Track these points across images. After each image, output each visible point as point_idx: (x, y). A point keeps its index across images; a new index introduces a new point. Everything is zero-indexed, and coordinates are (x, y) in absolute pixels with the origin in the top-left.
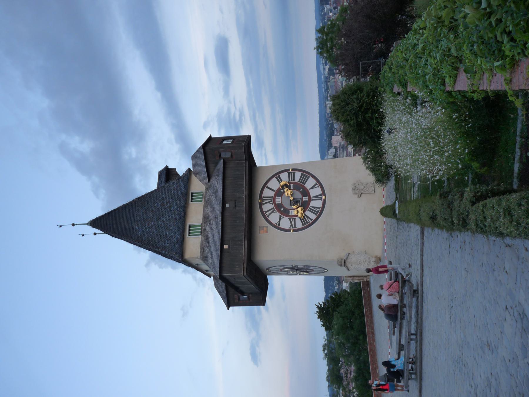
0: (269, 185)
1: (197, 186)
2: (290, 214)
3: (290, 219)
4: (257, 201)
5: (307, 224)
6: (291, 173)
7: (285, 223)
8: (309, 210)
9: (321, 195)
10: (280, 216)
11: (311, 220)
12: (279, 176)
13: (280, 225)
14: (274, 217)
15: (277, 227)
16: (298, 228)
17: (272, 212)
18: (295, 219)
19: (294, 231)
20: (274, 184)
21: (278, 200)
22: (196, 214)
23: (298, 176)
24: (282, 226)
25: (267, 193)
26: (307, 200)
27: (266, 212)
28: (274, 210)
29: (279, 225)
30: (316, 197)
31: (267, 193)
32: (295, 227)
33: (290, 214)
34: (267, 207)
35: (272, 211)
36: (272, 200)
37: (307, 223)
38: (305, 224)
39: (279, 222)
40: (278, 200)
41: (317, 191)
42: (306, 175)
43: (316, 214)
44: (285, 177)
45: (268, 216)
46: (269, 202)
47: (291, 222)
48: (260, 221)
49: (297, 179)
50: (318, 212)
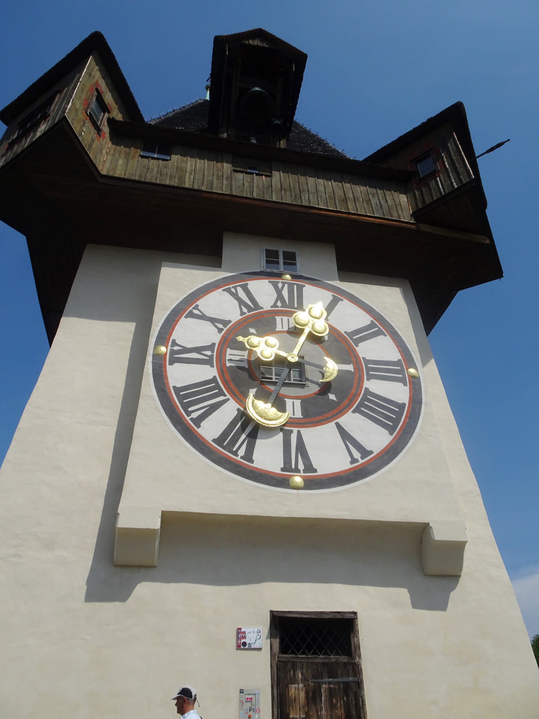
2: (229, 351)
9: (309, 468)
10: (225, 323)
11: (198, 421)
13: (190, 320)
17: (241, 302)
28: (250, 309)
30: (301, 447)
33: (229, 351)
37: (185, 407)
38: (181, 398)
39: (203, 317)
43: (219, 441)
45: (228, 291)
46: (280, 297)
47: (198, 350)
49: (375, 386)
50: (229, 447)
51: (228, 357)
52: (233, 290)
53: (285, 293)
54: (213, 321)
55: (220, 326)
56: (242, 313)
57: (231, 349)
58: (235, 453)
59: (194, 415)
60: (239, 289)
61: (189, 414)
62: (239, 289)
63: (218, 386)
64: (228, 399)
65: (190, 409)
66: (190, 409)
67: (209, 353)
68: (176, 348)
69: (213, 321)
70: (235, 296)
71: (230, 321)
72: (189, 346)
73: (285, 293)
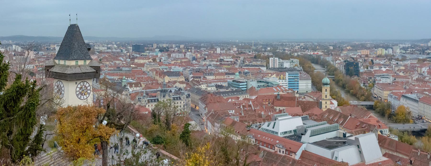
1: (88, 62)
4: (83, 81)
5: (77, 95)
7: (78, 89)
14: (79, 86)
15: (77, 87)
20: (87, 85)
21: (83, 87)
22: (81, 63)
23: (89, 92)
25: (85, 83)
31: (85, 83)
34: (82, 83)
36: (84, 84)
40: (83, 87)
41: (85, 97)
42: (89, 94)
48: (78, 82)
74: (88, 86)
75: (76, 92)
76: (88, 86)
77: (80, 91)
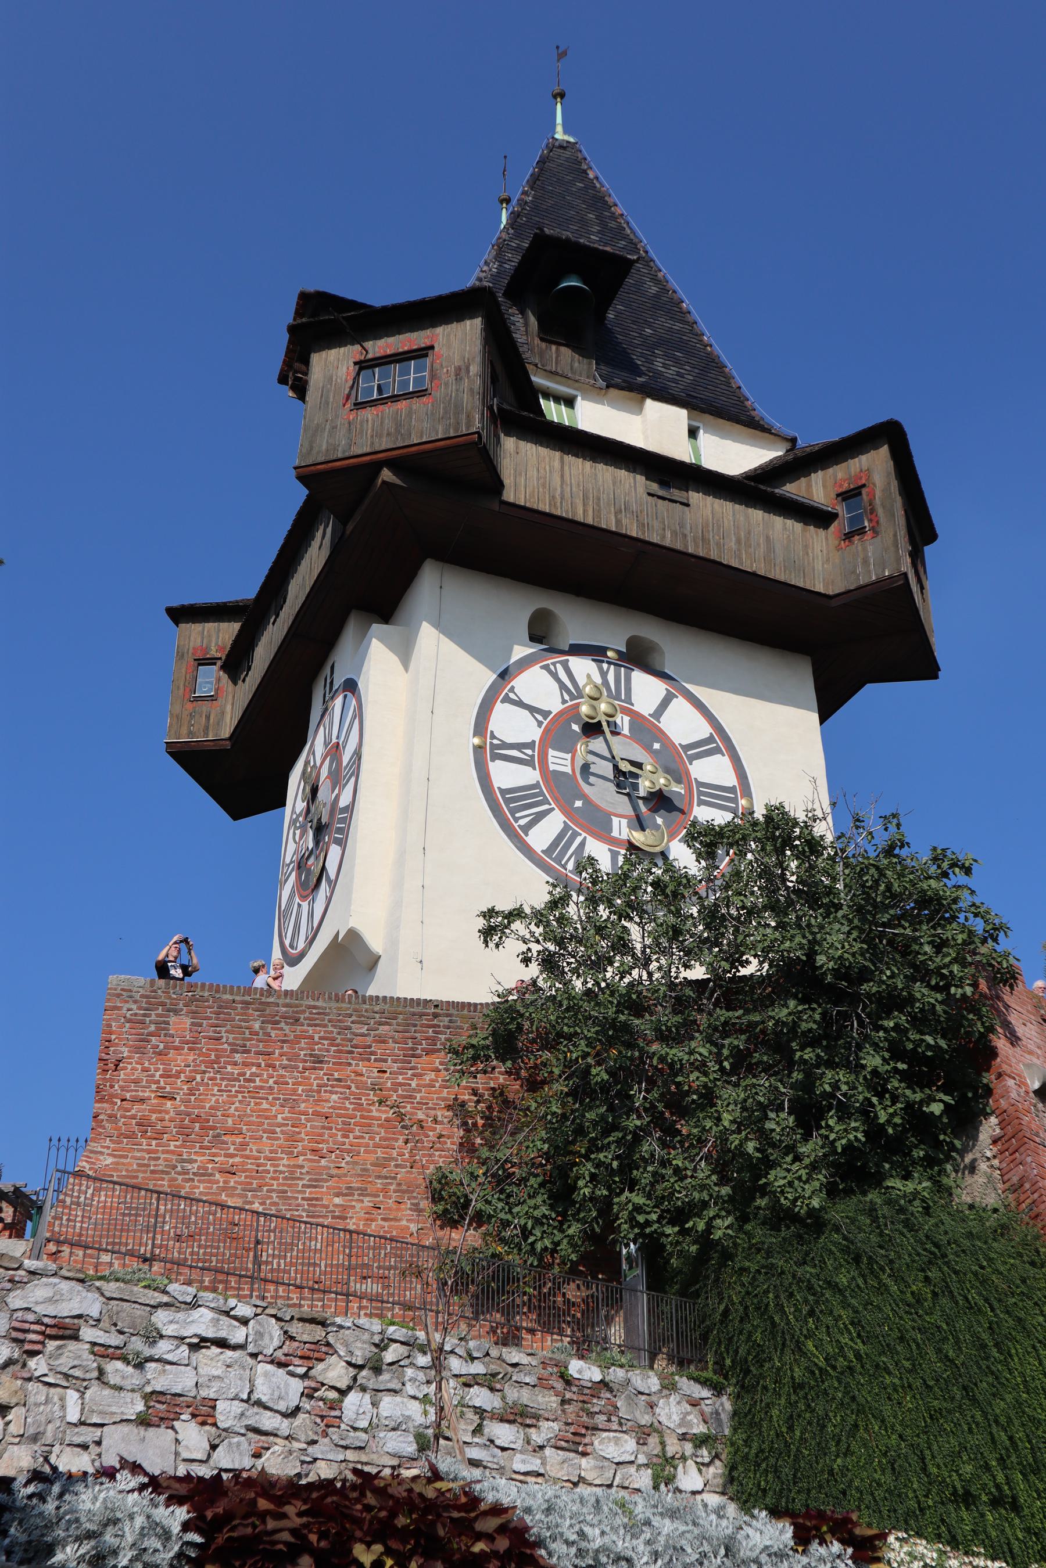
0: (680, 704)
2: (551, 752)
3: (531, 745)
6: (735, 800)
8: (566, 828)
10: (546, 714)
11: (526, 828)
12: (717, 751)
16: (491, 765)
17: (562, 686)
18: (529, 763)
19: (478, 749)
20: (682, 724)
24: (501, 710)
26: (615, 833)
27: (565, 665)
29: (507, 700)
32: (495, 757)
33: (551, 752)
35: (571, 690)
37: (513, 812)
38: (507, 801)
43: (548, 852)
44: (712, 770)
45: (546, 667)
51: (551, 760)
52: (552, 667)
53: (611, 677)
54: (532, 710)
55: (540, 718)
56: (564, 702)
57: (554, 749)
58: (564, 867)
59: (522, 822)
60: (558, 666)
61: (516, 820)
62: (558, 666)
63: (542, 793)
64: (553, 809)
65: (517, 815)
66: (517, 815)
67: (529, 752)
68: (495, 742)
69: (532, 710)
70: (555, 676)
71: (550, 712)
72: (509, 740)
73: (611, 677)
74: (703, 749)
75: (482, 757)
76: (703, 749)
77: (559, 761)
